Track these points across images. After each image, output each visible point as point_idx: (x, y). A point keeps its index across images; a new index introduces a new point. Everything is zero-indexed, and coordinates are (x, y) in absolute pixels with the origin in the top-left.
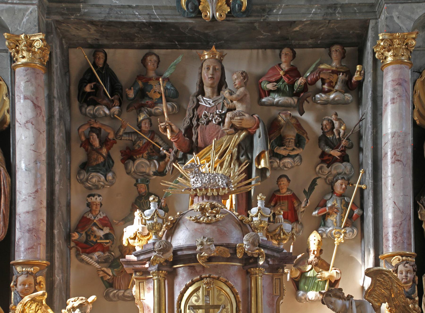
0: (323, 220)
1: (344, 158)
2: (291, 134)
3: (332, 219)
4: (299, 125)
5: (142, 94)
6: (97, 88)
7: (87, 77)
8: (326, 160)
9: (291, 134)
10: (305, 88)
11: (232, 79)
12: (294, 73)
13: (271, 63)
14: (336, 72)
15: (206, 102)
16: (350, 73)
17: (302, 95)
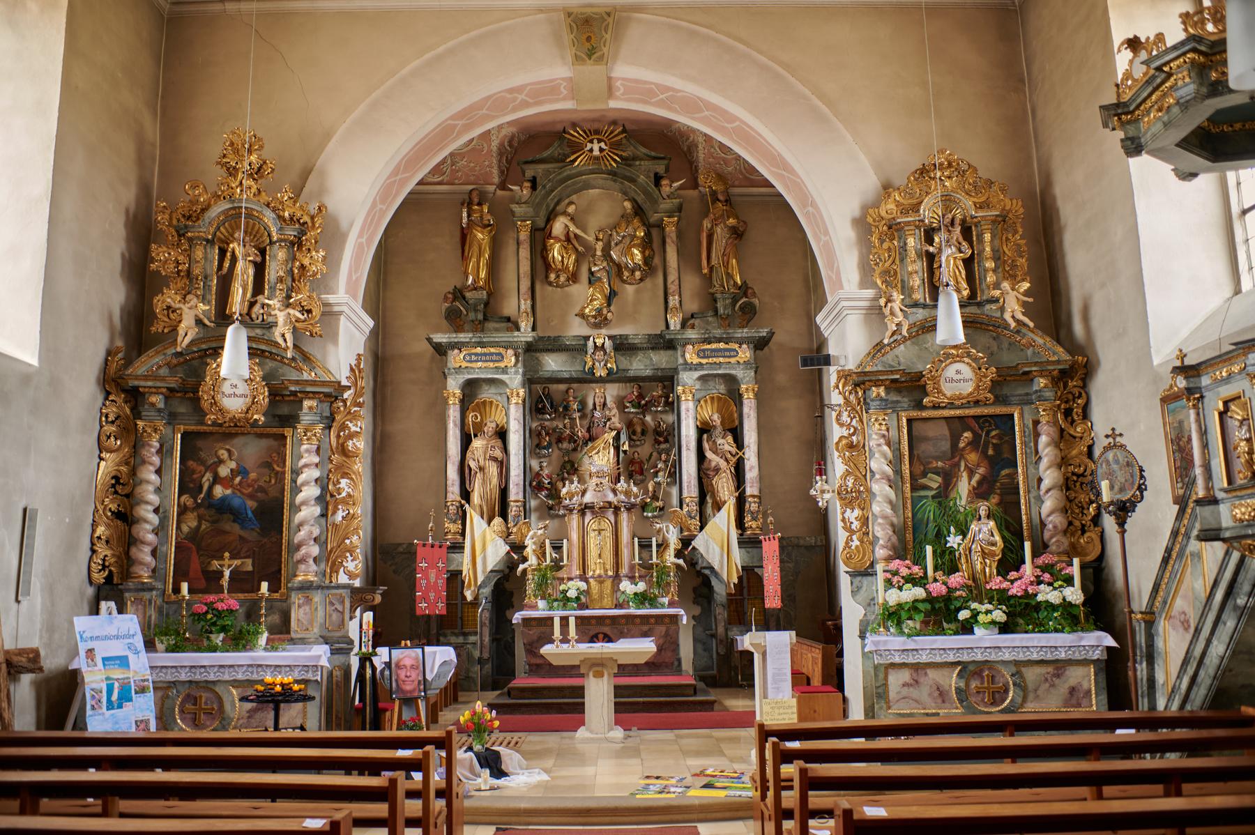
0: (656, 474)
1: (666, 441)
2: (639, 430)
3: (661, 474)
4: (644, 423)
5: (566, 408)
6: (544, 406)
7: (540, 400)
8: (659, 443)
9: (639, 430)
10: (646, 405)
11: (610, 403)
12: (641, 396)
13: (629, 391)
14: (660, 397)
15: (597, 414)
16: (668, 397)
17: (645, 409)
